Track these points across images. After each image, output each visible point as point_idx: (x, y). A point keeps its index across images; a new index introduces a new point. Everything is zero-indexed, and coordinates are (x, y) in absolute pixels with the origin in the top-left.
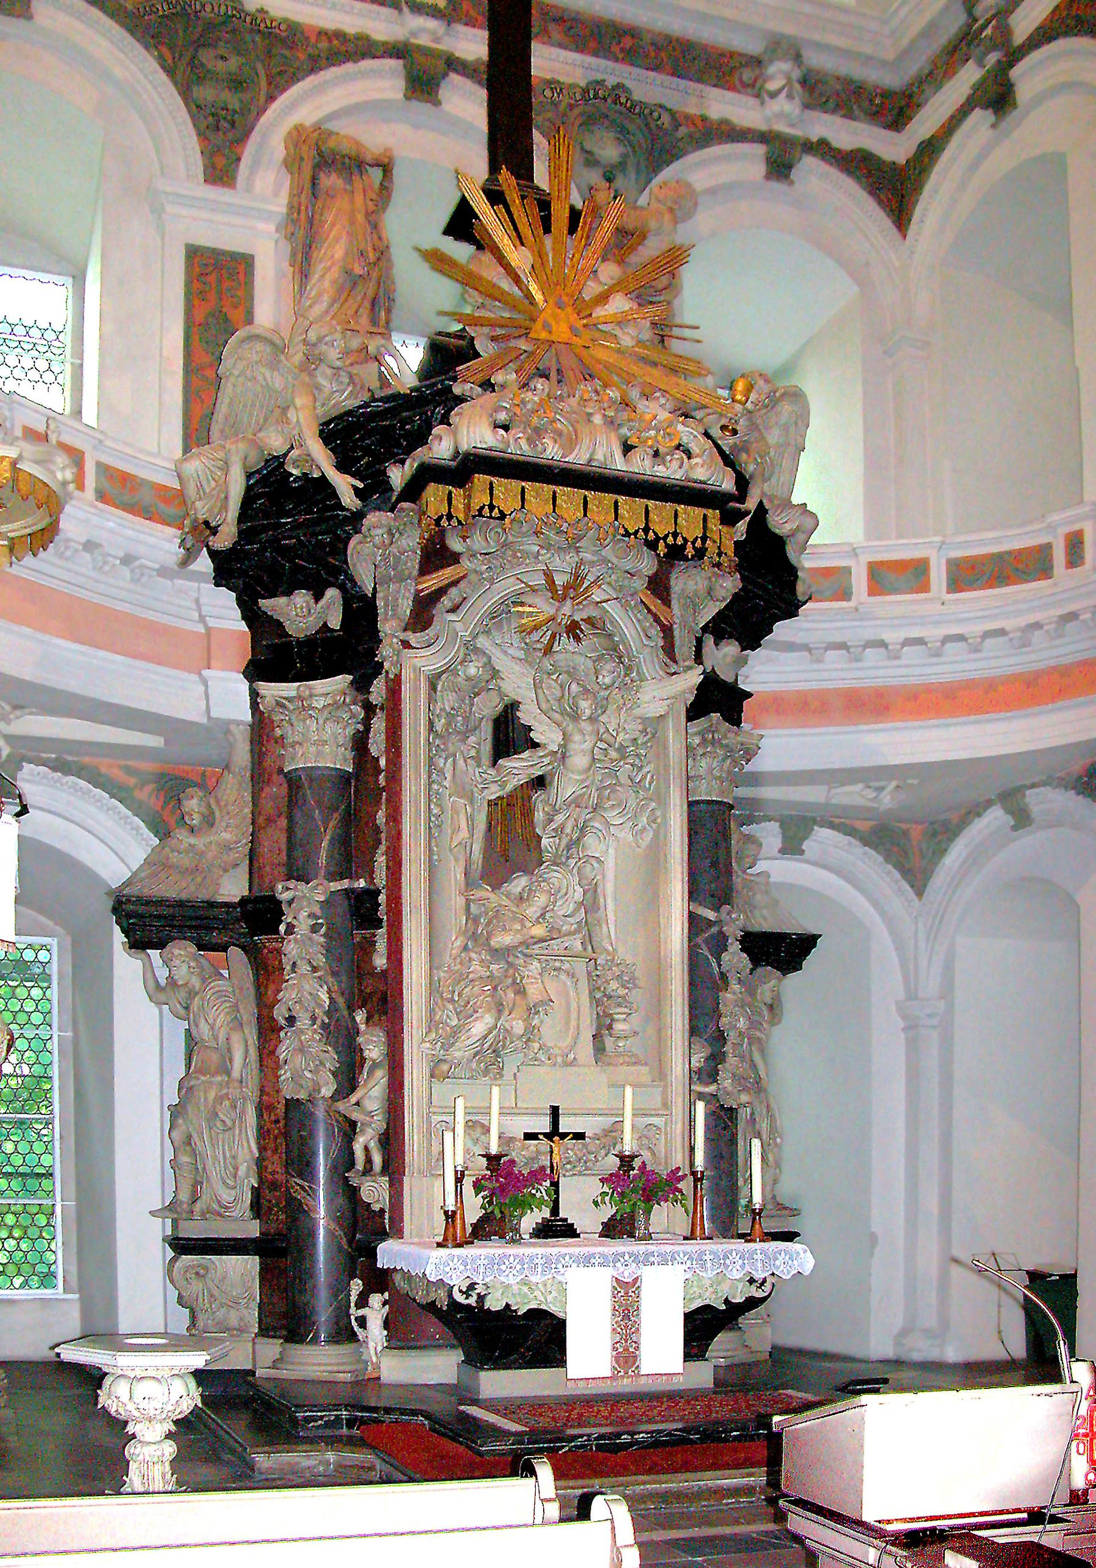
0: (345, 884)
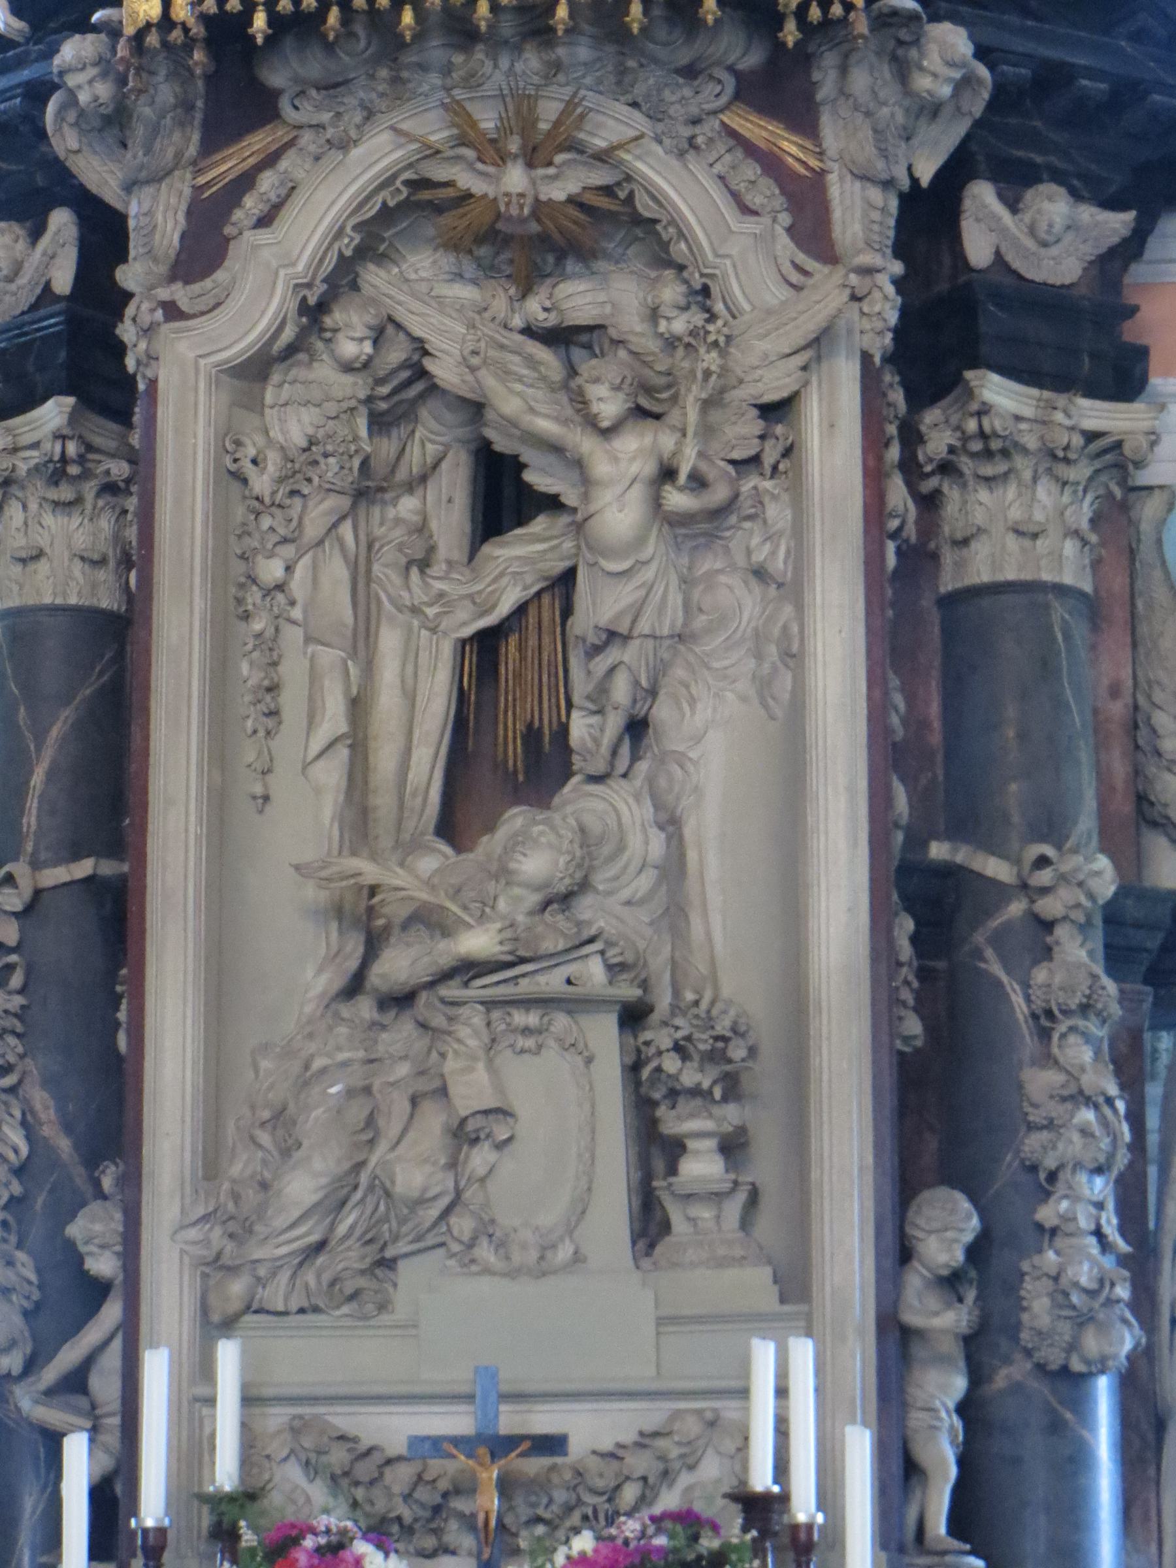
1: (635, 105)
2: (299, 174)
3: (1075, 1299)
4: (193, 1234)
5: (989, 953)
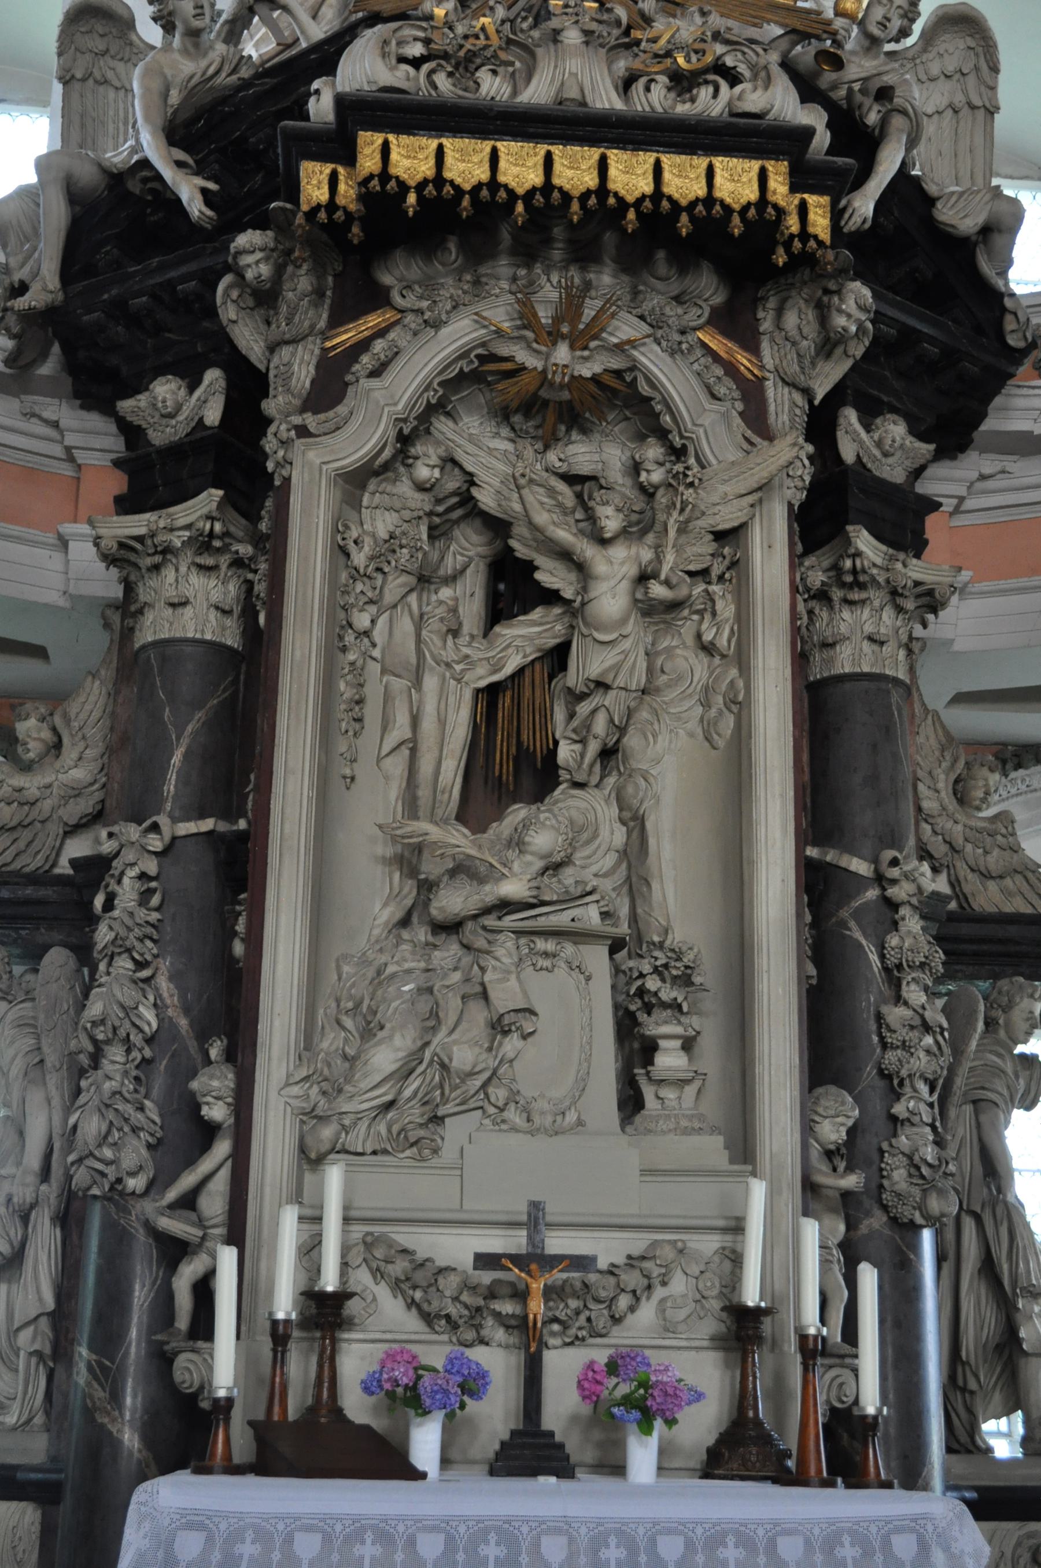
1: (642, 317)
2: (402, 343)
3: (925, 1171)
4: (296, 1090)
5: (852, 924)
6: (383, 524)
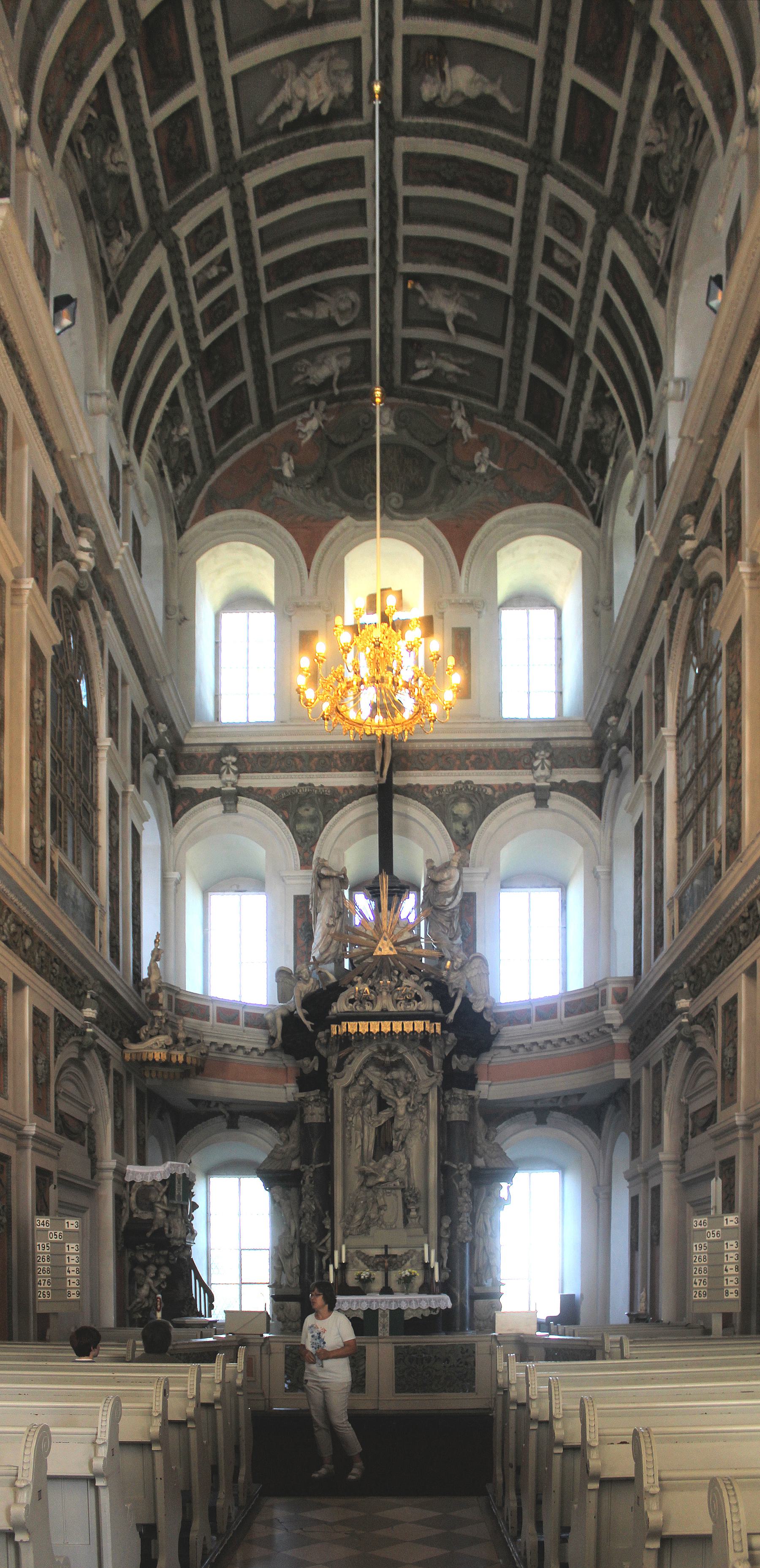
0: (322, 1165)
6: (353, 1095)
